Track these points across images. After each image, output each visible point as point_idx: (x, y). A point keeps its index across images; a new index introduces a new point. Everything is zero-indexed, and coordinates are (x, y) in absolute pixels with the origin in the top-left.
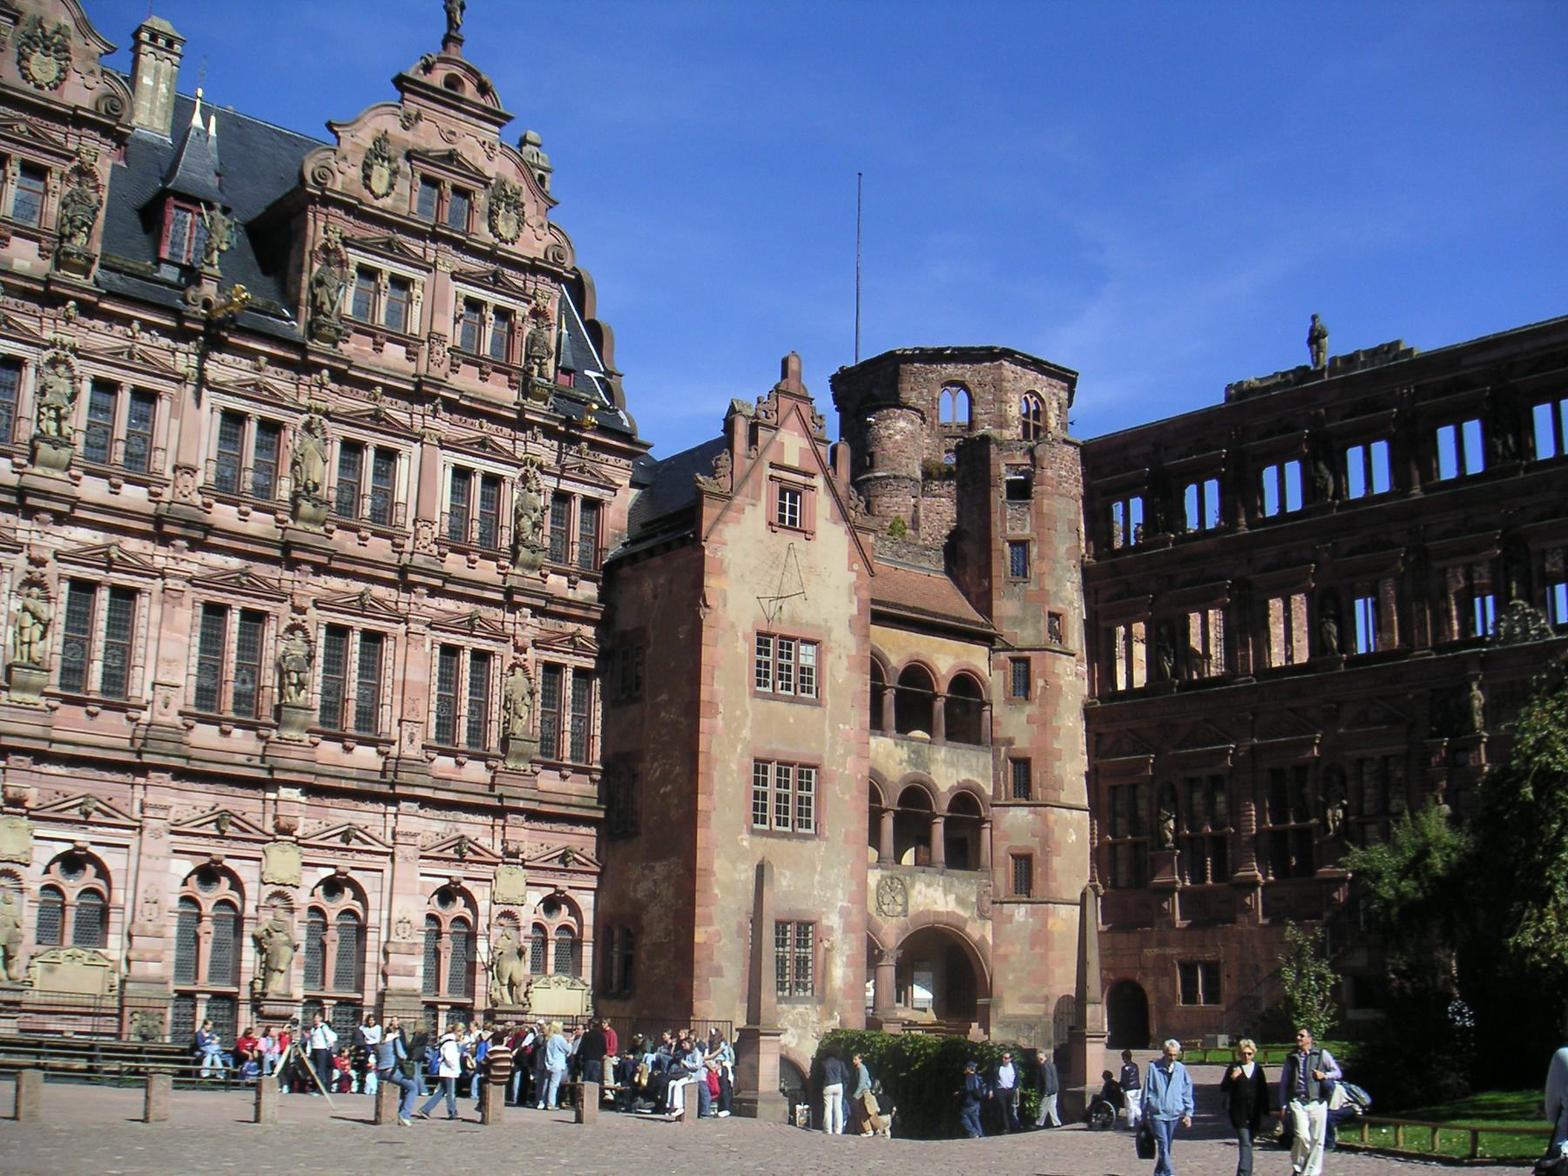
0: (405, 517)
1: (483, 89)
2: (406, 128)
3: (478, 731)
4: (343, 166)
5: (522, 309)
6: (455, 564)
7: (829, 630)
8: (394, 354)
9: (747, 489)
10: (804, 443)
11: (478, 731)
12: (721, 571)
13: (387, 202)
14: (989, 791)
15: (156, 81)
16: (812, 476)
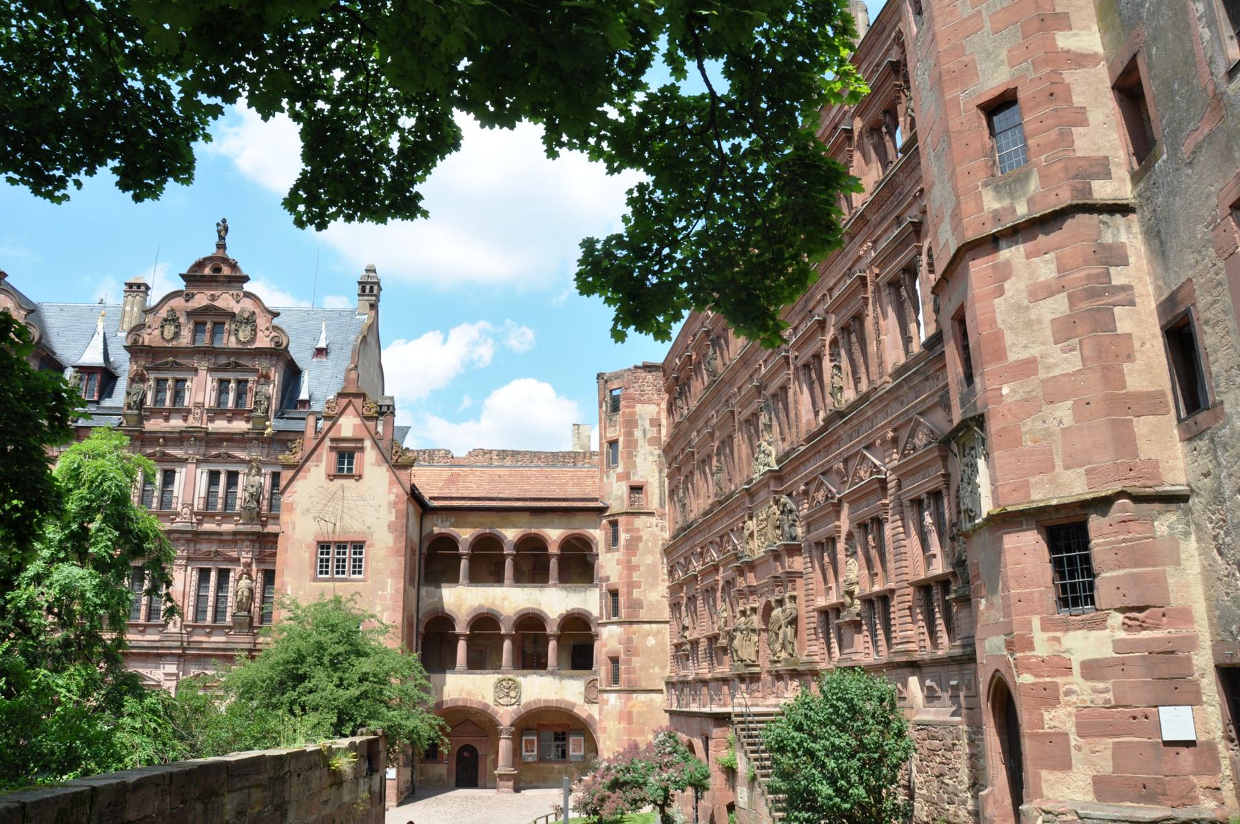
0: (178, 506)
1: (234, 266)
2: (187, 301)
3: (218, 613)
4: (149, 331)
5: (252, 378)
6: (208, 526)
7: (372, 534)
8: (176, 423)
9: (314, 457)
10: (358, 421)
11: (218, 613)
12: (291, 508)
13: (174, 343)
14: (595, 612)
15: (132, 308)
16: (362, 440)
